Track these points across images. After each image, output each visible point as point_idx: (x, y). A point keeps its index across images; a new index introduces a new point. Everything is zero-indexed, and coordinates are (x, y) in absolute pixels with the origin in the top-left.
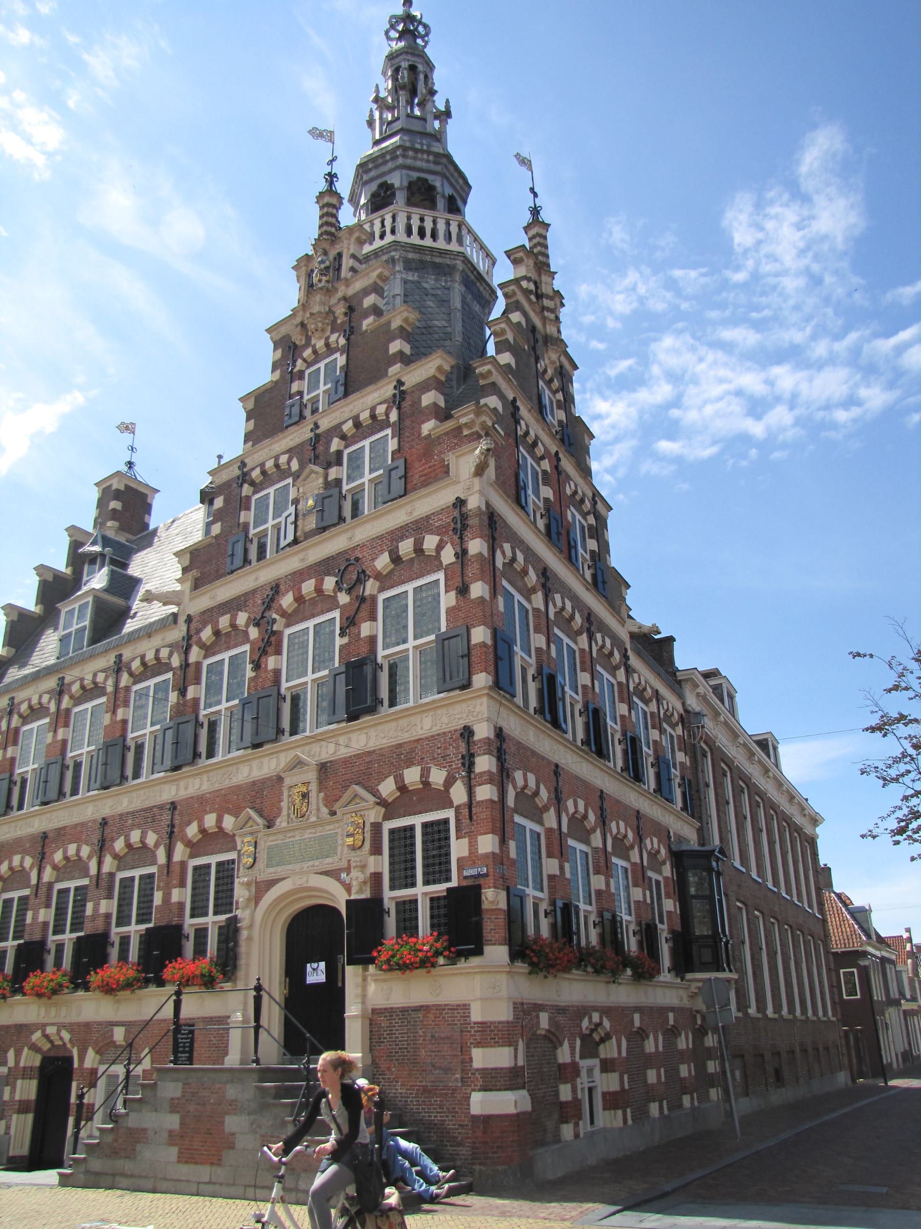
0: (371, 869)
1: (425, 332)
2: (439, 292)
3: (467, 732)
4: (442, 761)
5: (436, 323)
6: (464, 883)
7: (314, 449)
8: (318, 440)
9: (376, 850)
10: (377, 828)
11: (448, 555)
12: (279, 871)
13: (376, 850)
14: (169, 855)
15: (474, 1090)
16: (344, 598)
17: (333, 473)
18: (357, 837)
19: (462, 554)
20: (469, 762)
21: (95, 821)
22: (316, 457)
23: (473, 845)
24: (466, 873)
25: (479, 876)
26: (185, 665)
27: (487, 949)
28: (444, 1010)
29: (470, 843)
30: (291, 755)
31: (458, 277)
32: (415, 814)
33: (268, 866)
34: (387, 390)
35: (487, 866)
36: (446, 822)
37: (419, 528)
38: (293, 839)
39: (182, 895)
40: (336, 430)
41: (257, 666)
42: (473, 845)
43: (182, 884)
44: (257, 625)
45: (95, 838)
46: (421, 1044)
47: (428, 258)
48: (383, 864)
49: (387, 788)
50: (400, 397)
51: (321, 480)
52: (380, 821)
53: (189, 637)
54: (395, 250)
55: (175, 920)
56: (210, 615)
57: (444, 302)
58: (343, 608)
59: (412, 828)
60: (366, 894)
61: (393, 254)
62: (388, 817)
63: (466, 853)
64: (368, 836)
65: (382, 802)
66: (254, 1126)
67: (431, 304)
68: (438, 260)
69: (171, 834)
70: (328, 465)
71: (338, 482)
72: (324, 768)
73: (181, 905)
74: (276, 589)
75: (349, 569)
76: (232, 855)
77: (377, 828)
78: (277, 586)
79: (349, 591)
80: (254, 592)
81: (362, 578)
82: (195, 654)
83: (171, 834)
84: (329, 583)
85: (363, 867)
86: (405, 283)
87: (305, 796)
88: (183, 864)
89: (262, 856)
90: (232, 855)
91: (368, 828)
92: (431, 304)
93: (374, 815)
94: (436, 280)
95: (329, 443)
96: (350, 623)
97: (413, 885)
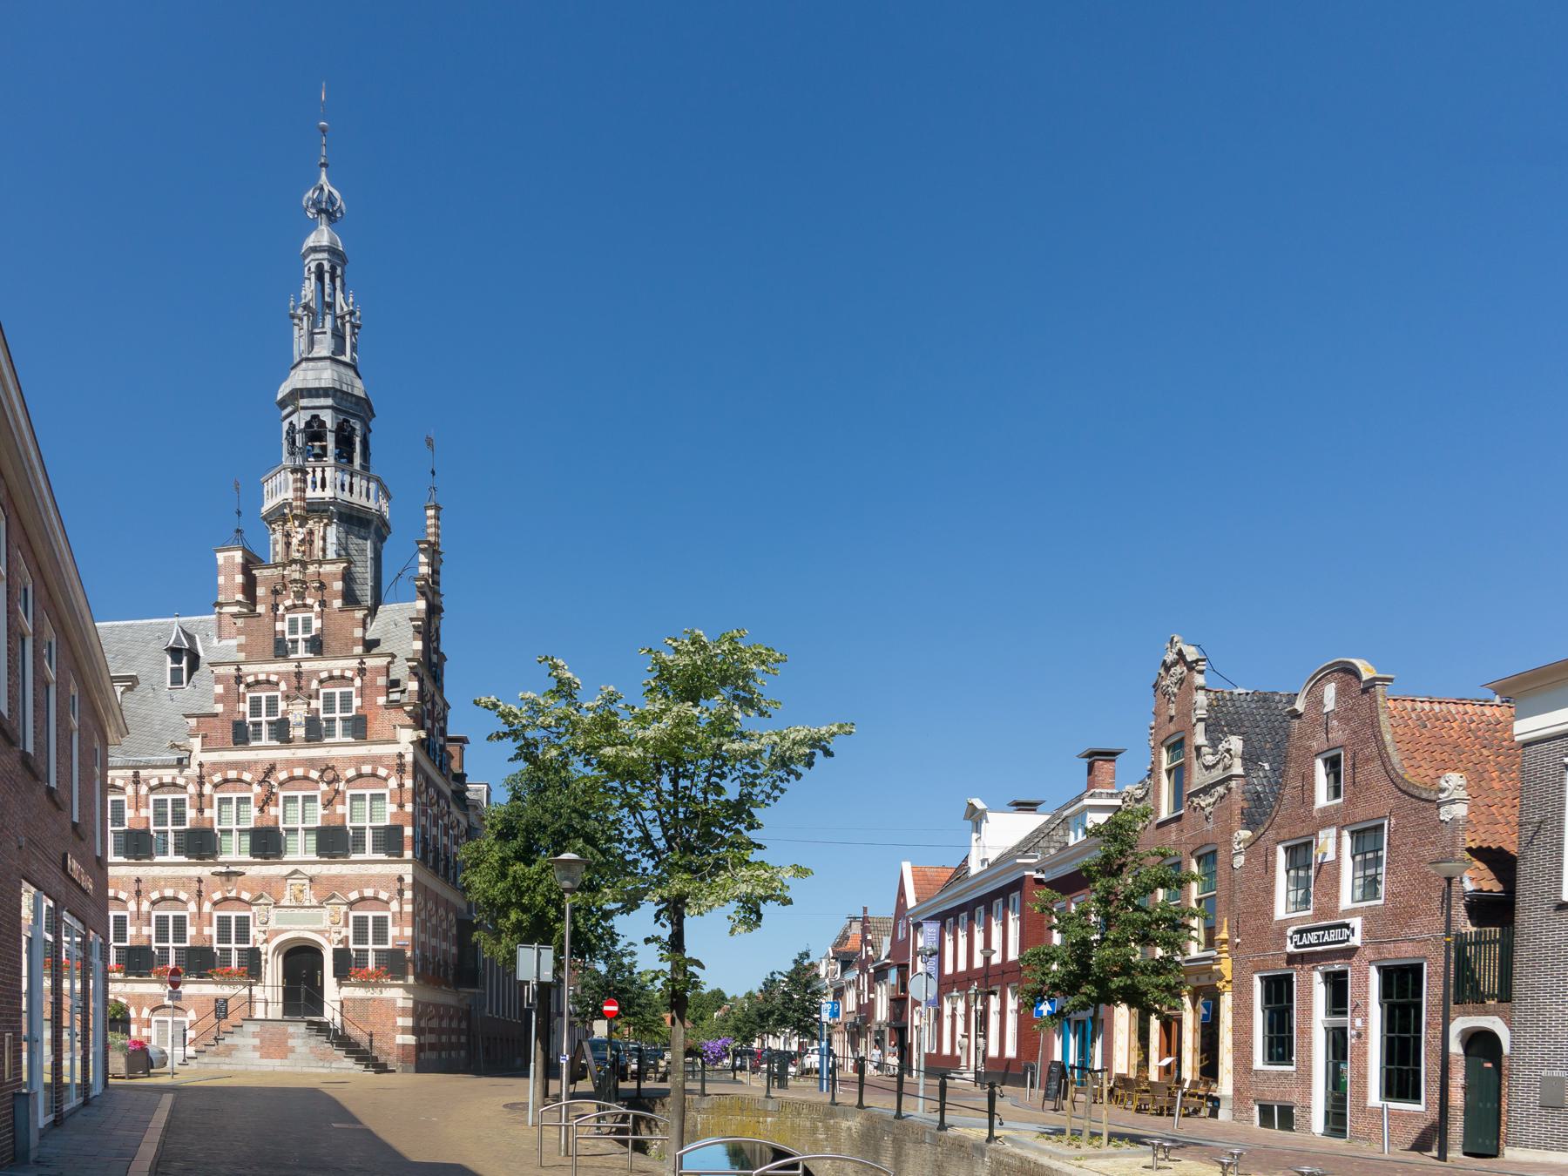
3: (401, 879)
4: (386, 888)
11: (393, 783)
14: (200, 908)
16: (324, 787)
17: (314, 704)
19: (401, 786)
20: (401, 892)
21: (129, 877)
26: (201, 795)
34: (355, 663)
37: (376, 760)
39: (212, 931)
40: (316, 672)
42: (401, 932)
43: (211, 925)
44: (260, 783)
45: (134, 888)
48: (350, 932)
50: (362, 671)
53: (201, 777)
56: (217, 766)
58: (323, 794)
70: (310, 697)
73: (211, 937)
75: (328, 771)
77: (346, 914)
79: (329, 783)
80: (256, 762)
81: (336, 779)
82: (207, 789)
84: (314, 774)
88: (210, 915)
93: (344, 908)
95: (309, 681)
96: (328, 803)
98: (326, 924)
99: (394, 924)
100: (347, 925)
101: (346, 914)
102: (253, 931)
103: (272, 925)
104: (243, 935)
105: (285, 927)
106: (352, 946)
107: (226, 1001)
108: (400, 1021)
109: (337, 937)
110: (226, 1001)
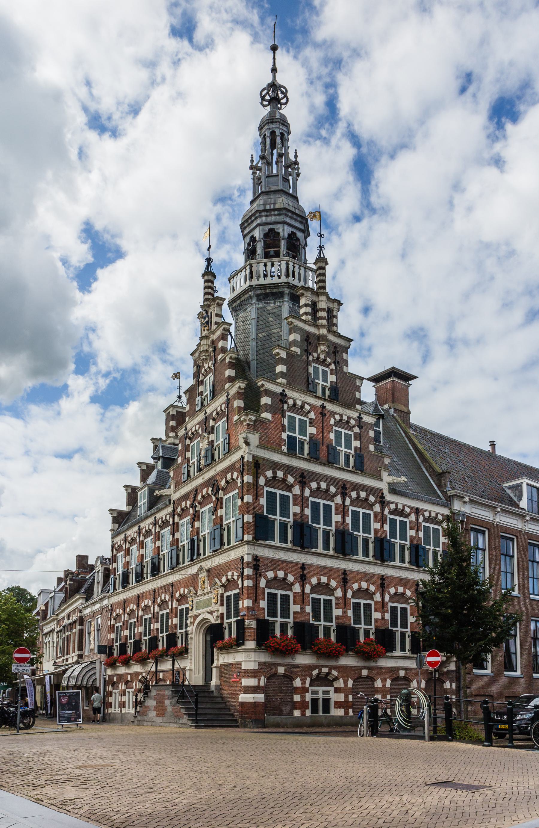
0: (220, 612)
1: (268, 338)
2: (276, 311)
5: (274, 331)
7: (205, 424)
8: (206, 420)
9: (222, 605)
10: (222, 595)
12: (199, 612)
13: (222, 605)
22: (206, 429)
30: (199, 565)
31: (286, 298)
41: (192, 527)
47: (268, 291)
48: (223, 610)
49: (224, 580)
51: (207, 441)
54: (251, 291)
57: (278, 316)
60: (218, 622)
61: (250, 293)
62: (225, 591)
64: (219, 598)
65: (223, 586)
67: (271, 319)
68: (274, 291)
69: (172, 596)
71: (213, 441)
72: (208, 571)
74: (196, 491)
77: (222, 595)
78: (197, 490)
83: (172, 596)
86: (258, 309)
87: (204, 582)
89: (194, 606)
91: (219, 595)
92: (271, 319)
93: (221, 591)
94: (275, 303)
96: (215, 511)
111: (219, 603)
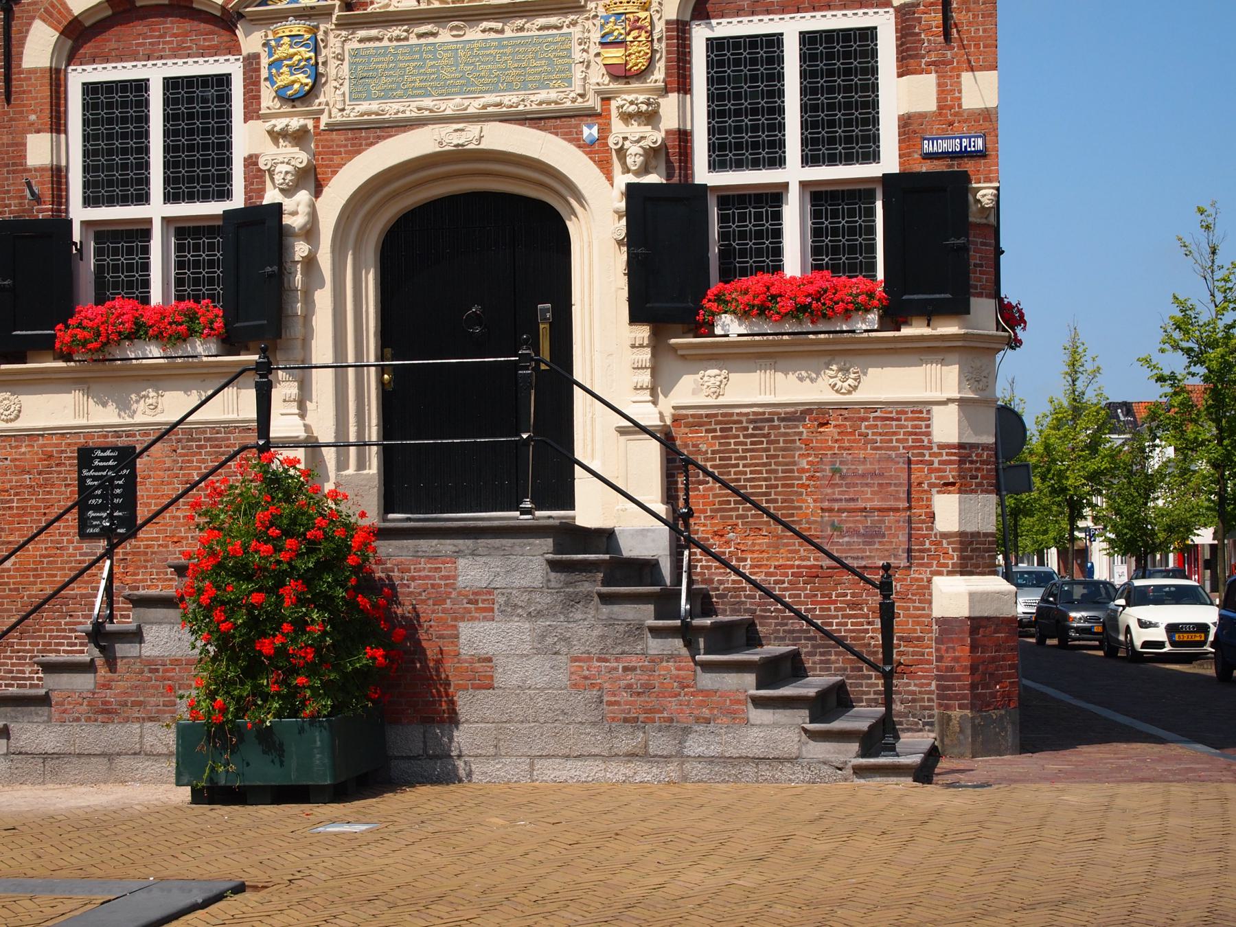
0: (670, 118)
6: (925, 167)
15: (940, 573)
18: (633, 49)
23: (948, 95)
24: (928, 147)
25: (963, 154)
27: (974, 302)
28: (867, 419)
29: (939, 85)
32: (783, 10)
33: (356, 97)
35: (984, 137)
36: (869, 34)
38: (431, 40)
42: (948, 95)
43: (58, 125)
46: (802, 486)
52: (688, 18)
55: (43, 212)
59: (775, 41)
63: (929, 104)
64: (661, 47)
66: (549, 640)
73: (58, 175)
76: (232, 67)
85: (650, 117)
90: (232, 67)
97: (778, 161)
98: (587, 78)
99: (907, 63)
100: (681, 82)
101: (680, 31)
102: (246, 138)
103: (336, 103)
104: (201, 149)
105: (393, 109)
106: (703, 175)
107: (127, 456)
108: (948, 512)
109: (635, 138)
110: (127, 456)
111: (659, 74)
